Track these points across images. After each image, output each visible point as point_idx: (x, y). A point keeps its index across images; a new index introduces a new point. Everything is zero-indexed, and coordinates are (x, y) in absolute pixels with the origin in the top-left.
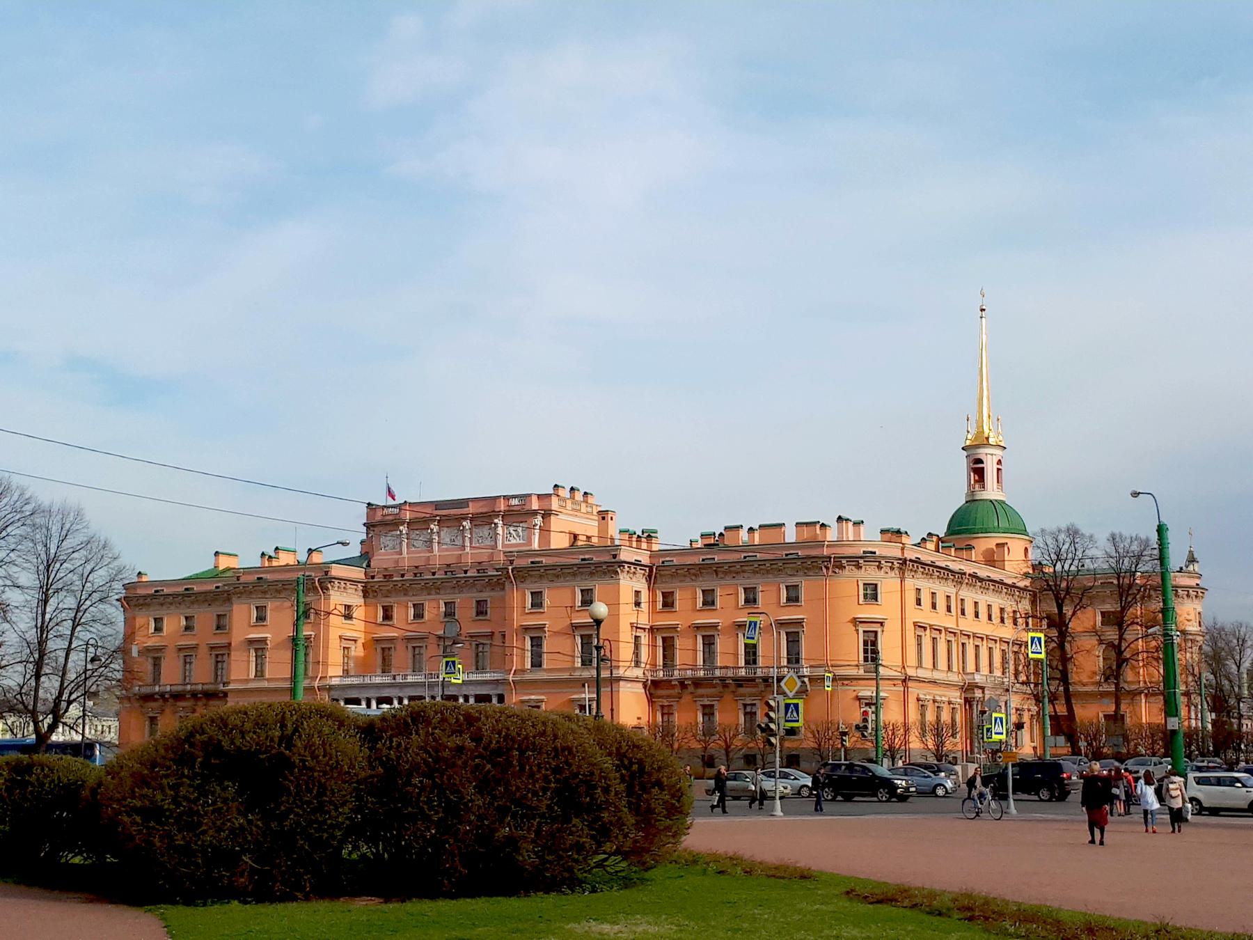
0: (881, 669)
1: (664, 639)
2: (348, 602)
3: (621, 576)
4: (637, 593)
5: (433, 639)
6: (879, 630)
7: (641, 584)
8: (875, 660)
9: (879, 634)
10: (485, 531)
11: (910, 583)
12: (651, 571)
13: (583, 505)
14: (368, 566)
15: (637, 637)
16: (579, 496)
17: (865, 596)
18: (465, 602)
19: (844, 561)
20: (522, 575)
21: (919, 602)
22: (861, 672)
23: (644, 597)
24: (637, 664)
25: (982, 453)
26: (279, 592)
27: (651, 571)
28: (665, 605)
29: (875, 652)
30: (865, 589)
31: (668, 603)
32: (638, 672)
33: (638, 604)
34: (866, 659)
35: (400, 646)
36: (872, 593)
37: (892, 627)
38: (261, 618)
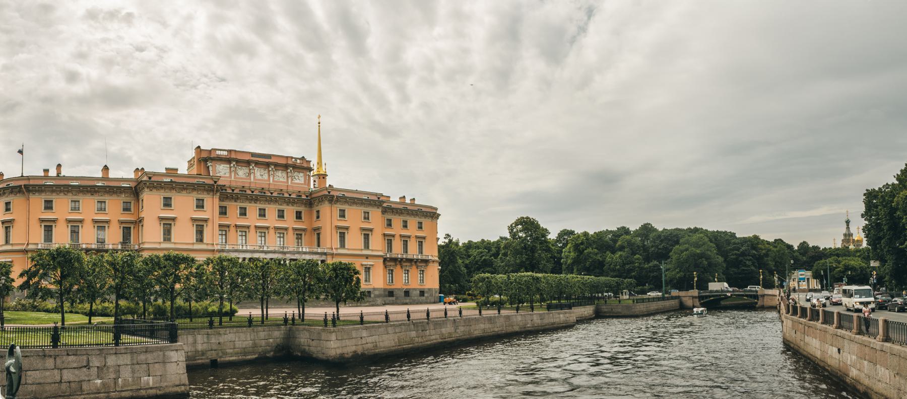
5: (252, 229)
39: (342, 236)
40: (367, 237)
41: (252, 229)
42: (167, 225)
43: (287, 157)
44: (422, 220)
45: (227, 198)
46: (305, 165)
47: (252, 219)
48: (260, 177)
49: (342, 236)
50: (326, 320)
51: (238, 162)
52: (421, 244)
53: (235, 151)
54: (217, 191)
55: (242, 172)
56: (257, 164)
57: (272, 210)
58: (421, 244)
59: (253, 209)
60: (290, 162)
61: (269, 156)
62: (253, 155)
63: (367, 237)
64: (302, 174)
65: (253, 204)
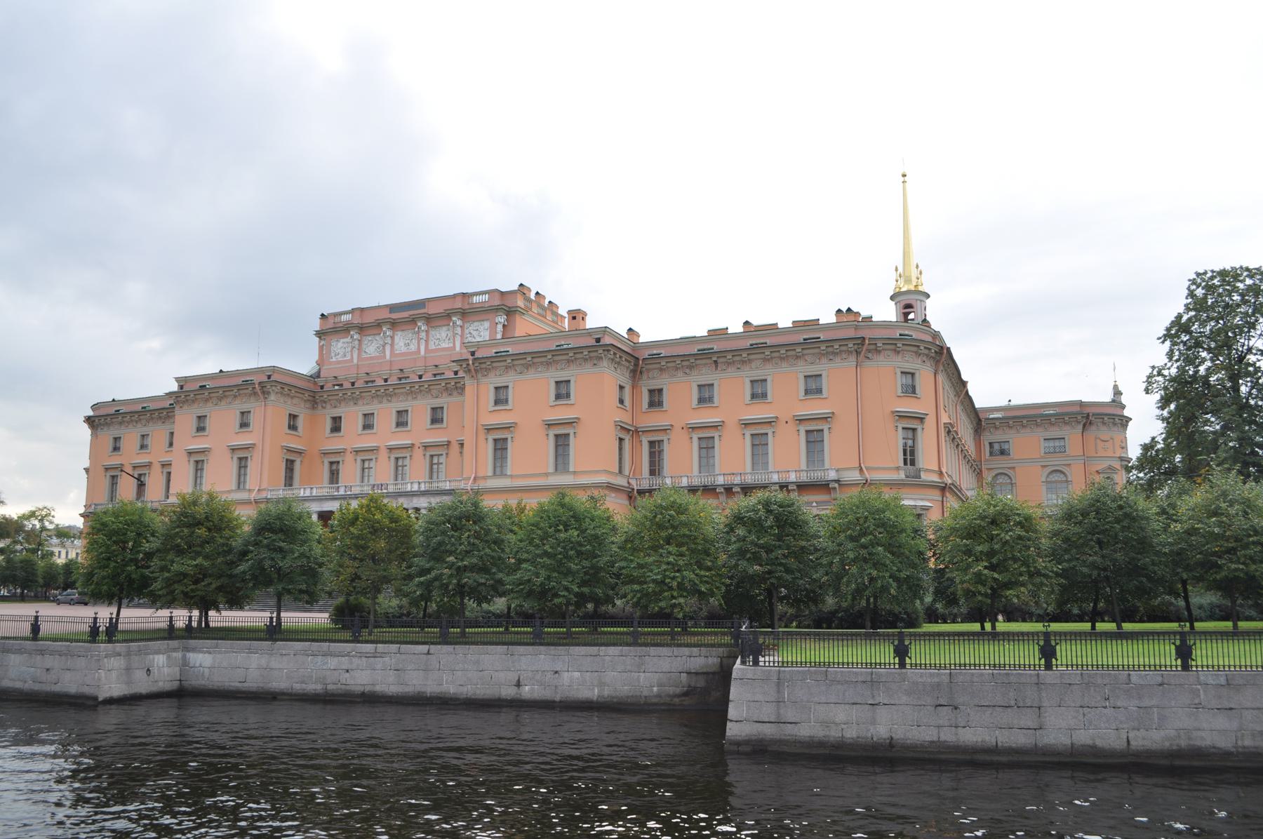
0: (922, 474)
1: (652, 443)
2: (295, 411)
4: (621, 388)
5: (383, 454)
6: (919, 428)
8: (913, 463)
9: (919, 431)
12: (636, 365)
13: (549, 313)
15: (621, 440)
18: (419, 410)
22: (902, 475)
24: (620, 471)
26: (220, 399)
27: (636, 365)
28: (652, 404)
29: (913, 453)
32: (621, 481)
34: (905, 463)
35: (349, 458)
37: (930, 422)
38: (201, 429)
39: (500, 447)
40: (562, 442)
41: (383, 454)
42: (198, 461)
43: (455, 296)
44: (821, 367)
45: (340, 401)
46: (497, 302)
47: (386, 434)
48: (404, 349)
49: (500, 447)
50: (94, 631)
51: (362, 329)
52: (814, 441)
53: (362, 310)
54: (269, 393)
55: (372, 347)
56: (394, 324)
57: (419, 410)
58: (814, 441)
59: (385, 413)
60: (458, 304)
61: (421, 304)
62: (393, 308)
63: (562, 442)
64: (487, 324)
65: (385, 405)
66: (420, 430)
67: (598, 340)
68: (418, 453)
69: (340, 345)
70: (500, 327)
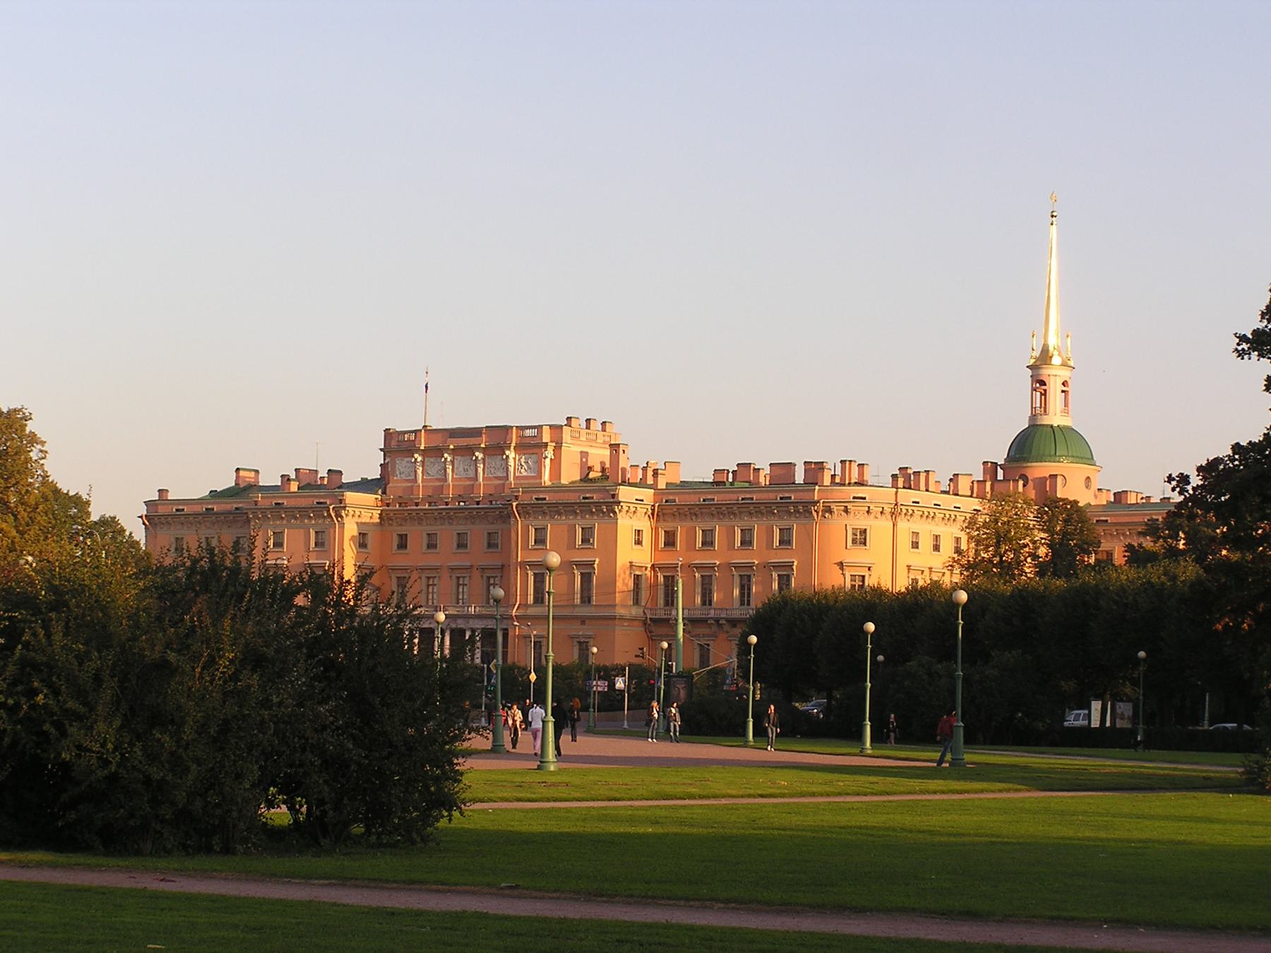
3: (619, 516)
7: (645, 525)
10: (497, 461)
11: (904, 526)
14: (384, 492)
16: (596, 426)
17: (854, 542)
19: (833, 506)
20: (525, 510)
21: (915, 545)
23: (647, 538)
24: (637, 602)
25: (1045, 372)
30: (854, 534)
31: (670, 542)
33: (639, 542)
36: (861, 538)
66: (477, 554)
67: (613, 496)
68: (477, 574)
69: (404, 463)
70: (548, 461)
